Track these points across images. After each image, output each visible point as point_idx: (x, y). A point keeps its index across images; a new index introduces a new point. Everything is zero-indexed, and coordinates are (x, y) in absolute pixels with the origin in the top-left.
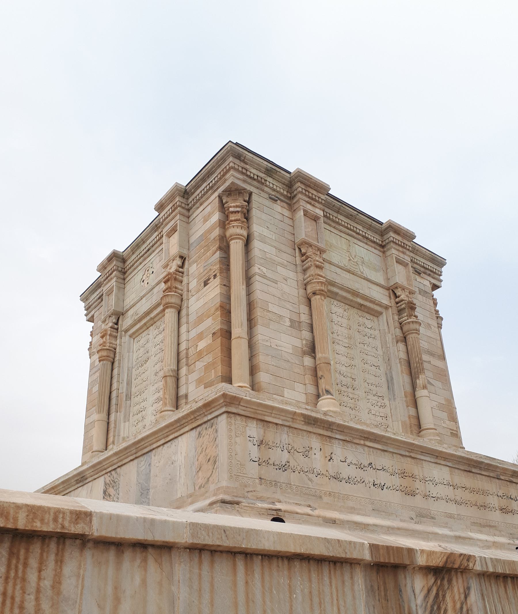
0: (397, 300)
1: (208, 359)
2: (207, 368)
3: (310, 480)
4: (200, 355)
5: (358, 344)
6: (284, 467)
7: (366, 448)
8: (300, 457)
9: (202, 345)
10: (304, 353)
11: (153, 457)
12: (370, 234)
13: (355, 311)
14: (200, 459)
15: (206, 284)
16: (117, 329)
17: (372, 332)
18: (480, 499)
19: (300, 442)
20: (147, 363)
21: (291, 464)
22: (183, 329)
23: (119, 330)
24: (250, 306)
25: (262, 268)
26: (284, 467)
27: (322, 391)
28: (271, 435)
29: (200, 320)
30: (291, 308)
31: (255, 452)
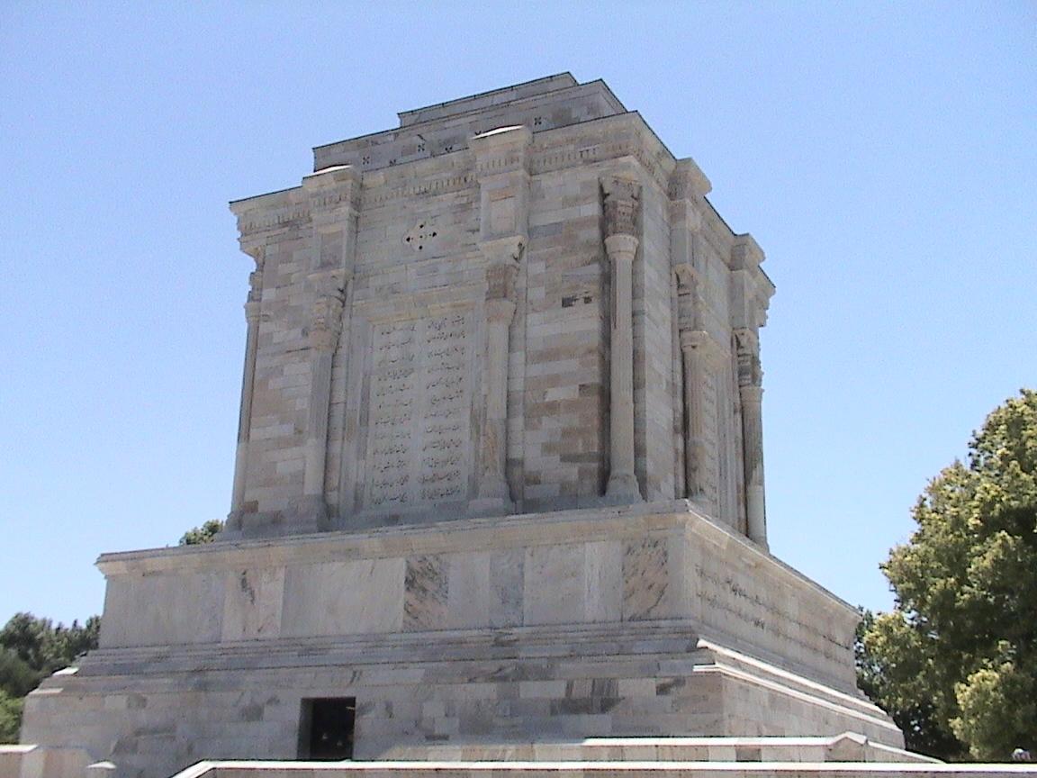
0: (740, 352)
1: (575, 421)
2: (566, 433)
4: (552, 407)
9: (554, 394)
10: (675, 429)
11: (527, 556)
14: (632, 581)
15: (567, 303)
16: (344, 302)
20: (412, 376)
22: (519, 357)
23: (347, 303)
24: (637, 359)
27: (696, 489)
29: (548, 355)
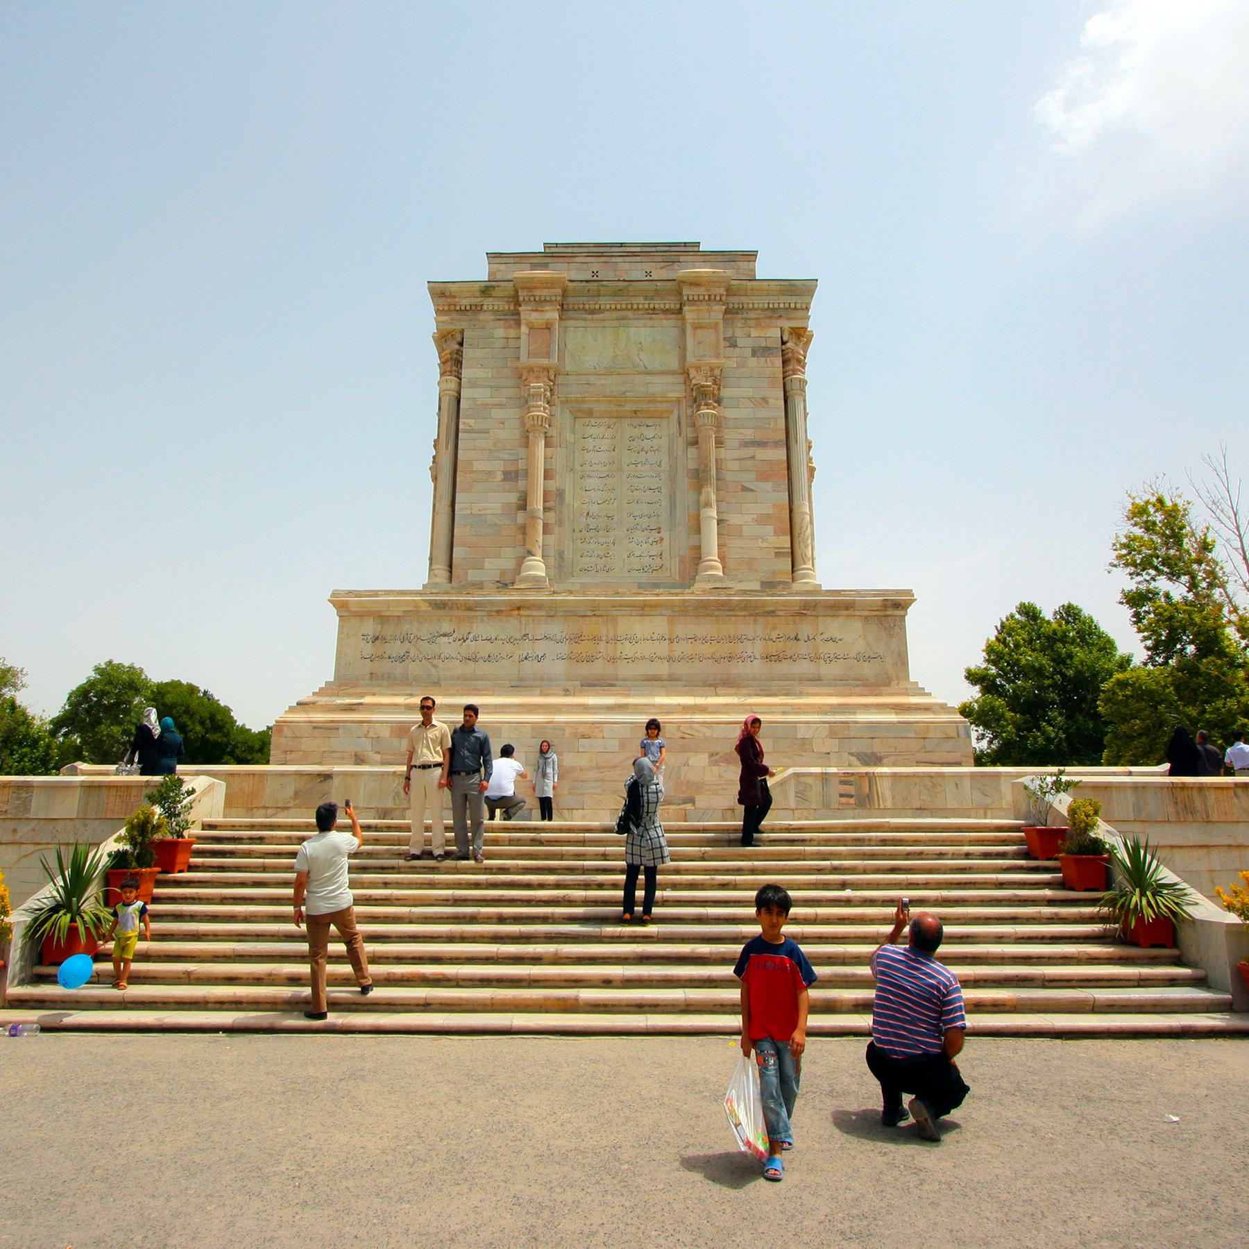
3: (434, 666)
5: (625, 468)
6: (402, 659)
7: (523, 619)
8: (425, 645)
12: (658, 304)
13: (628, 421)
17: (656, 442)
18: (725, 649)
19: (425, 630)
21: (411, 655)
25: (467, 421)
26: (402, 659)
28: (389, 631)
30: (506, 457)
31: (369, 649)
